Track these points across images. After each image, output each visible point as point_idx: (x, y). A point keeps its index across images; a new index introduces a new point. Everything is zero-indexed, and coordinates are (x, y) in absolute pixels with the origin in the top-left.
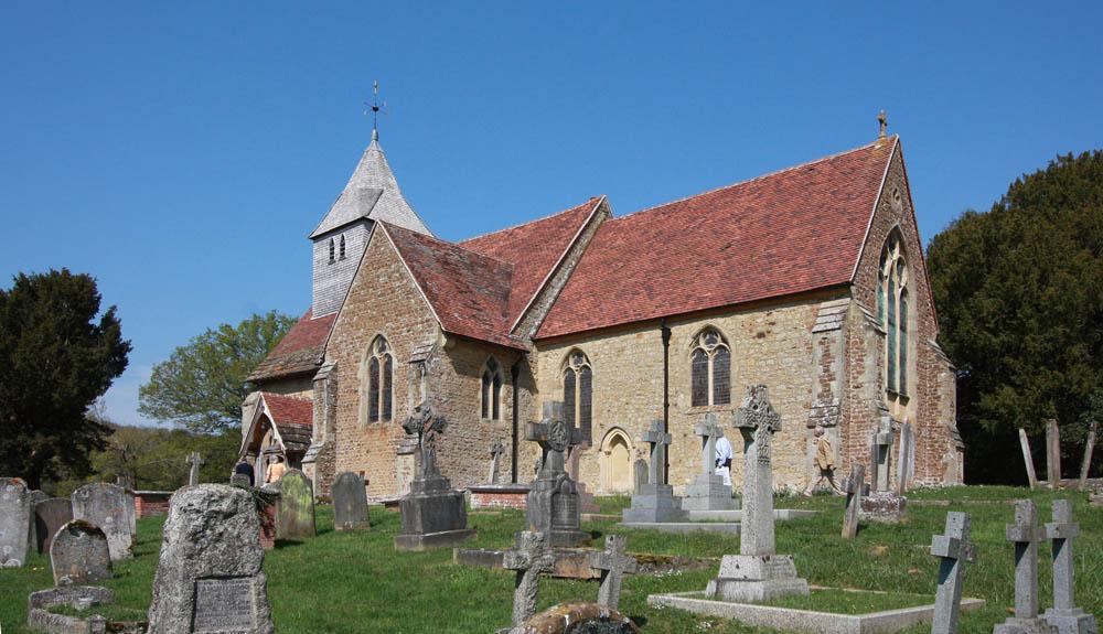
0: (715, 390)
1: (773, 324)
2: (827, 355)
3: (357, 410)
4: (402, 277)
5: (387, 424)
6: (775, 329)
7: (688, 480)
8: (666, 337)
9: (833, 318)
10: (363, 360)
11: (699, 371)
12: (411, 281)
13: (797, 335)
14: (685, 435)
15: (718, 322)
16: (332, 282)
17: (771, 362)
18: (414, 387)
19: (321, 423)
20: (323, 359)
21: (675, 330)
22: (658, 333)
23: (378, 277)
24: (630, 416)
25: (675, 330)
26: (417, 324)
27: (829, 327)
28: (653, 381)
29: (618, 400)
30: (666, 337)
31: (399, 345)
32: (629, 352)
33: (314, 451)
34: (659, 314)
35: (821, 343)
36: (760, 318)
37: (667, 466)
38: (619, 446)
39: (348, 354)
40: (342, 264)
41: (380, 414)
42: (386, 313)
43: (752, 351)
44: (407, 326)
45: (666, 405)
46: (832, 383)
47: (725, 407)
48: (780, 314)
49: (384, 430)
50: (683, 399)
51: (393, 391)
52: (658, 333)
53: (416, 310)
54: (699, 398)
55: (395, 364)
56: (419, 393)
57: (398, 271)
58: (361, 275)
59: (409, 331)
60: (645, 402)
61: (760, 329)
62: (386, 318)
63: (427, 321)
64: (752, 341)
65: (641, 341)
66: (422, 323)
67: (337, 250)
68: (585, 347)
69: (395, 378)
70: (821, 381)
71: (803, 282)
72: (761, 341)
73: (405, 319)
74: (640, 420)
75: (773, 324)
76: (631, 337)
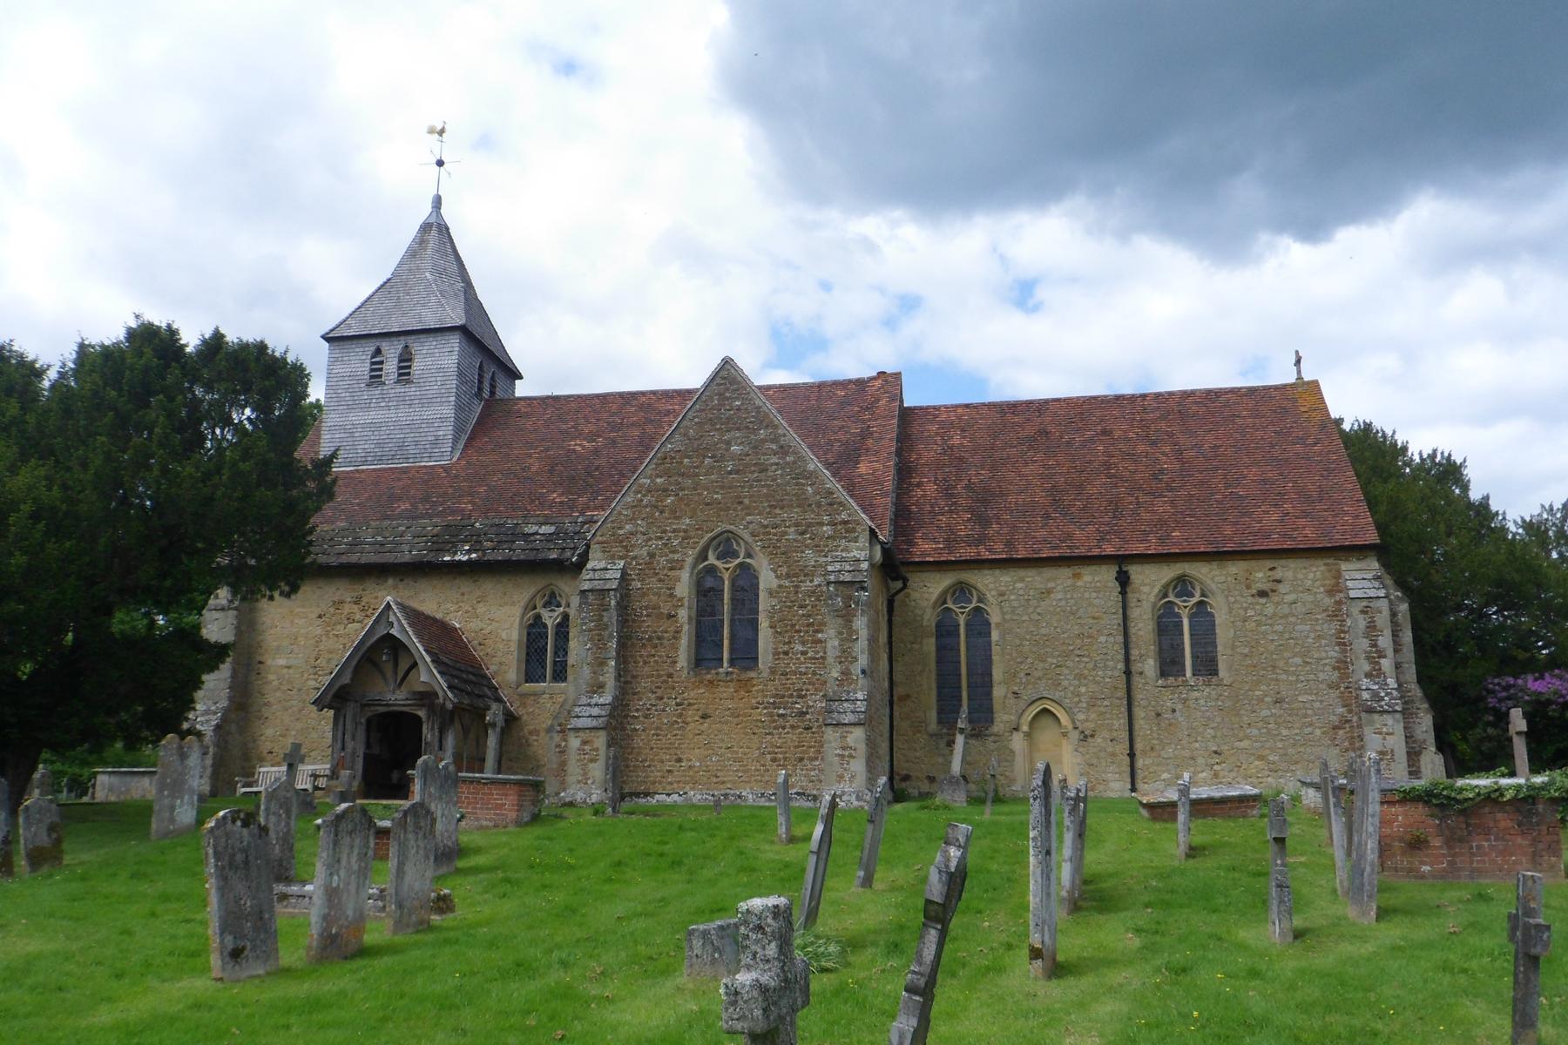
0: (1194, 657)
1: (1279, 581)
2: (1372, 627)
3: (675, 648)
4: (784, 450)
5: (752, 674)
6: (1282, 588)
7: (1165, 776)
8: (1124, 580)
9: (1366, 584)
10: (687, 568)
11: (1166, 626)
12: (802, 459)
13: (1310, 598)
14: (1158, 715)
15: (1202, 572)
16: (374, 415)
17: (1280, 628)
18: (840, 620)
19: (602, 663)
20: (584, 558)
21: (1136, 572)
22: (1108, 574)
23: (728, 443)
24: (1065, 683)
25: (1136, 572)
26: (821, 524)
27: (1372, 593)
28: (1102, 639)
29: (1044, 661)
30: (1124, 580)
31: (781, 554)
32: (1060, 596)
33: (596, 711)
34: (1109, 550)
35: (1362, 612)
36: (1260, 573)
37: (1132, 755)
38: (1046, 721)
39: (652, 555)
40: (411, 390)
41: (726, 656)
42: (747, 501)
43: (1250, 613)
44: (797, 525)
45: (1128, 673)
46: (1383, 661)
47: (1214, 680)
48: (1289, 570)
49: (746, 685)
50: (1150, 666)
51: (764, 623)
52: (1106, 575)
53: (819, 505)
54: (1169, 665)
55: (767, 579)
56: (851, 631)
57: (772, 441)
58: (685, 435)
59: (803, 533)
60: (1090, 666)
61: (1260, 586)
62: (748, 508)
63: (845, 522)
64: (1250, 599)
65: (1080, 583)
66: (833, 524)
67: (391, 367)
68: (987, 582)
69: (764, 602)
70: (1368, 658)
71: (1308, 534)
72: (1263, 600)
73: (795, 513)
74: (1083, 690)
75: (1279, 581)
76: (1064, 573)
